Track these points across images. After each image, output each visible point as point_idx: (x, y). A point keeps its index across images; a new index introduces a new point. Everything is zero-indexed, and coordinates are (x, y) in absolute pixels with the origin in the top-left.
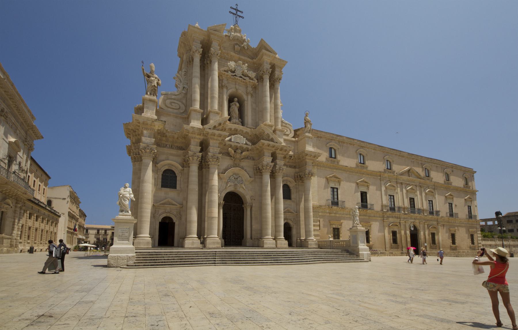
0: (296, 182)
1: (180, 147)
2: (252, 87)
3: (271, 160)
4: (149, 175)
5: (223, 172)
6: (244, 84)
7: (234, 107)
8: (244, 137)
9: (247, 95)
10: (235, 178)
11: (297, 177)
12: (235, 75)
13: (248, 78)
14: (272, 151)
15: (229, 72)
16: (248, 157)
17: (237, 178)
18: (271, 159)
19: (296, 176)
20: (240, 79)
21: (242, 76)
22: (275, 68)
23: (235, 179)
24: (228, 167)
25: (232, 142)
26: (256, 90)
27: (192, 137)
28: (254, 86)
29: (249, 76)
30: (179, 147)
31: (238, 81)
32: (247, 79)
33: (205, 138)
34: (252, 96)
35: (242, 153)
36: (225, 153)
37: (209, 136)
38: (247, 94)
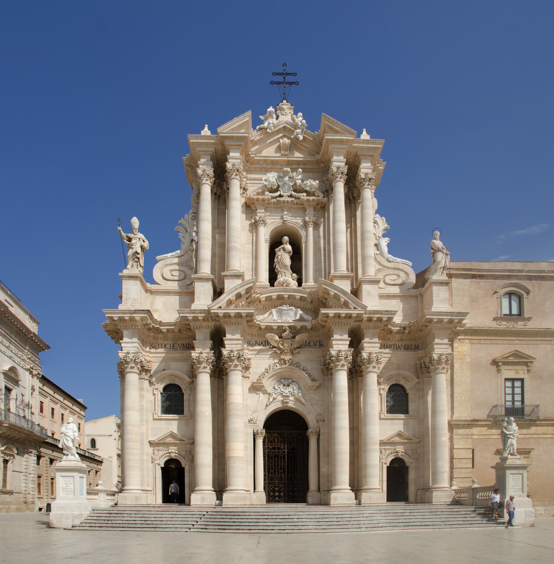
0: (418, 379)
2: (315, 209)
4: (133, 398)
6: (299, 206)
8: (296, 308)
11: (421, 368)
12: (280, 196)
13: (305, 194)
14: (349, 327)
16: (309, 343)
19: (418, 366)
20: (290, 199)
21: (293, 193)
27: (195, 327)
29: (307, 190)
32: (303, 196)
33: (217, 323)
35: (294, 337)
36: (264, 343)
37: (221, 320)
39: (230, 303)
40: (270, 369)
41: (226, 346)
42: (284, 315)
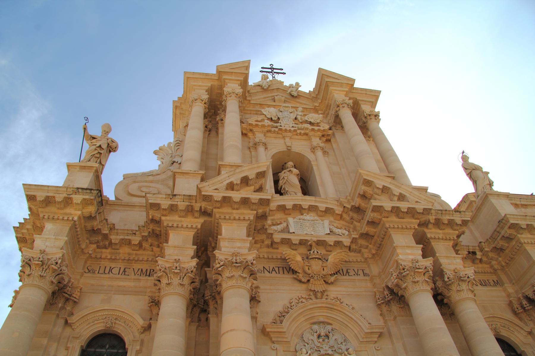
1: (147, 270)
3: (421, 252)
5: (275, 320)
7: (287, 175)
9: (313, 152)
10: (319, 336)
15: (266, 121)
16: (347, 272)
17: (327, 336)
18: (417, 251)
22: (360, 105)
23: (321, 340)
24: (291, 303)
25: (291, 233)
26: (331, 144)
28: (324, 139)
30: (144, 271)
31: (289, 134)
34: (325, 153)
36: (277, 269)
38: (313, 149)
39: (231, 186)
40: (292, 308)
41: (223, 249)
42: (307, 228)
